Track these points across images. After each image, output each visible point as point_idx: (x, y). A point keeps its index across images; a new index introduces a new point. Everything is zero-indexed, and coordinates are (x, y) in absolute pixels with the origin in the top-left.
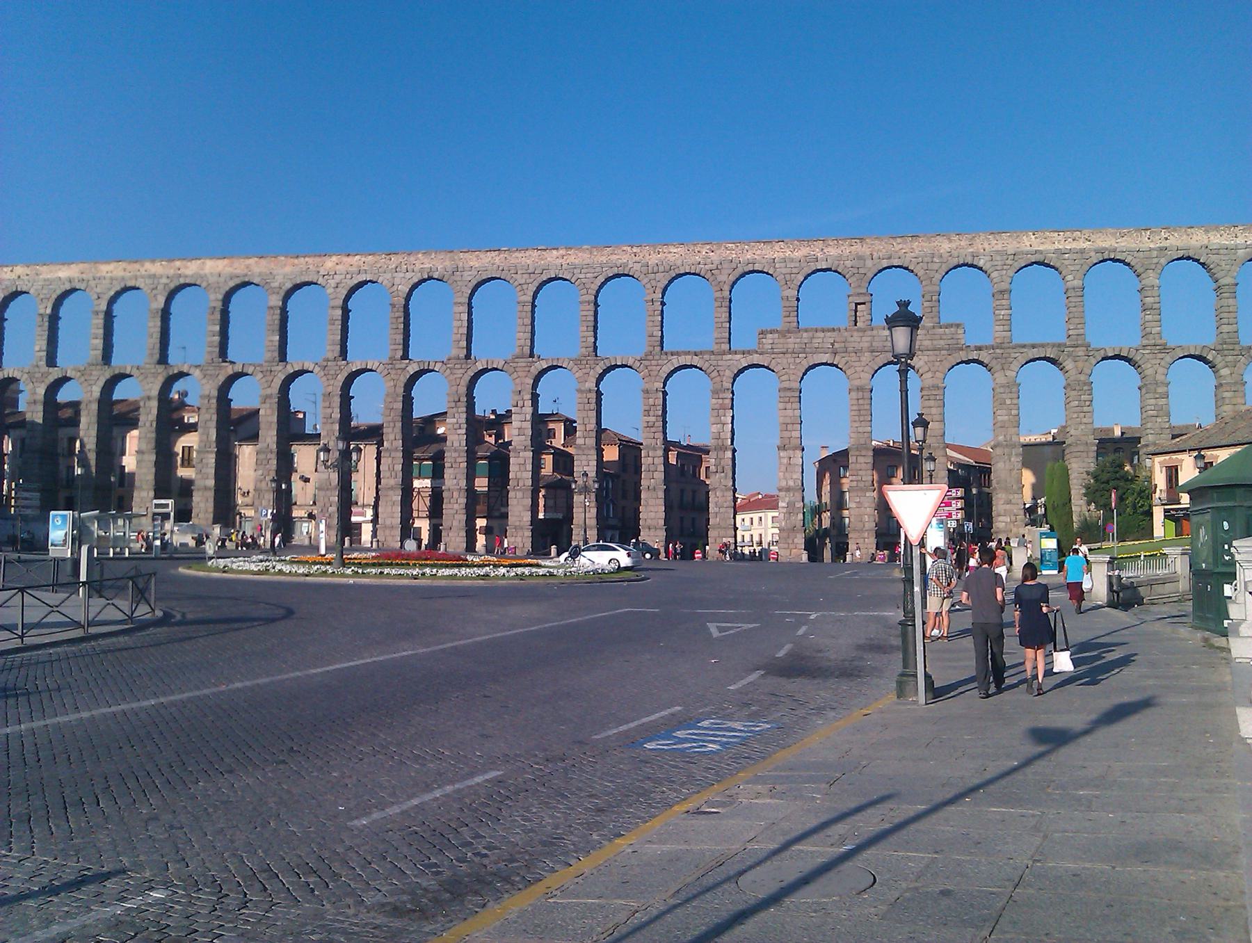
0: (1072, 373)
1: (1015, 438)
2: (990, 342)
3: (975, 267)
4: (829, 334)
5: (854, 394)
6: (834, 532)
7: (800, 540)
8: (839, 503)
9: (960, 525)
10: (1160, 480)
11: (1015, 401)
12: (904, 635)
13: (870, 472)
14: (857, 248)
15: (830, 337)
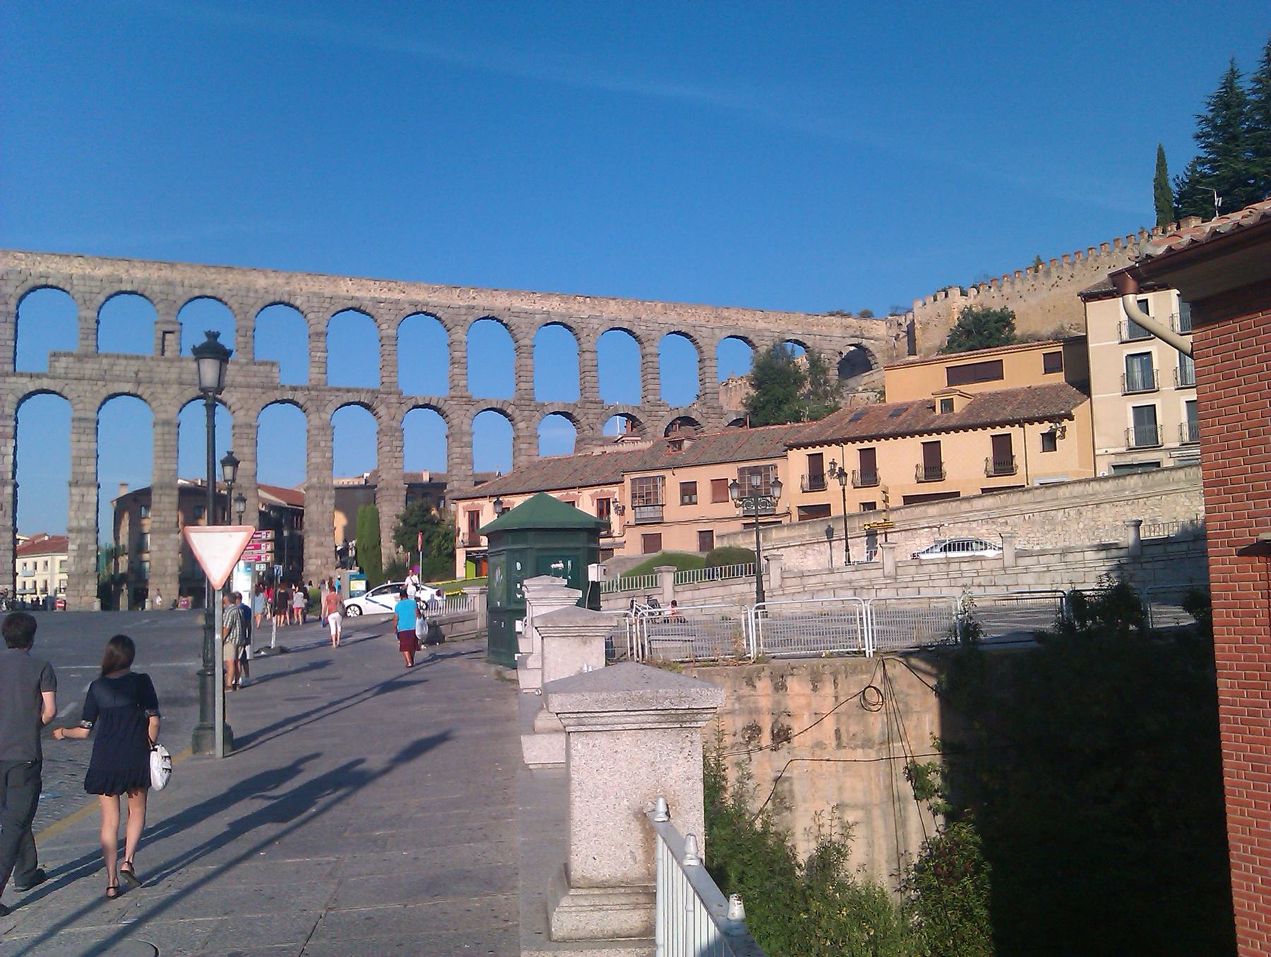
0: (385, 418)
1: (328, 481)
2: (305, 383)
3: (292, 306)
4: (133, 362)
5: (159, 429)
6: (132, 578)
7: (92, 587)
8: (138, 545)
9: (270, 568)
10: (463, 524)
11: (329, 444)
12: (203, 687)
13: (174, 513)
14: (166, 273)
15: (134, 366)
